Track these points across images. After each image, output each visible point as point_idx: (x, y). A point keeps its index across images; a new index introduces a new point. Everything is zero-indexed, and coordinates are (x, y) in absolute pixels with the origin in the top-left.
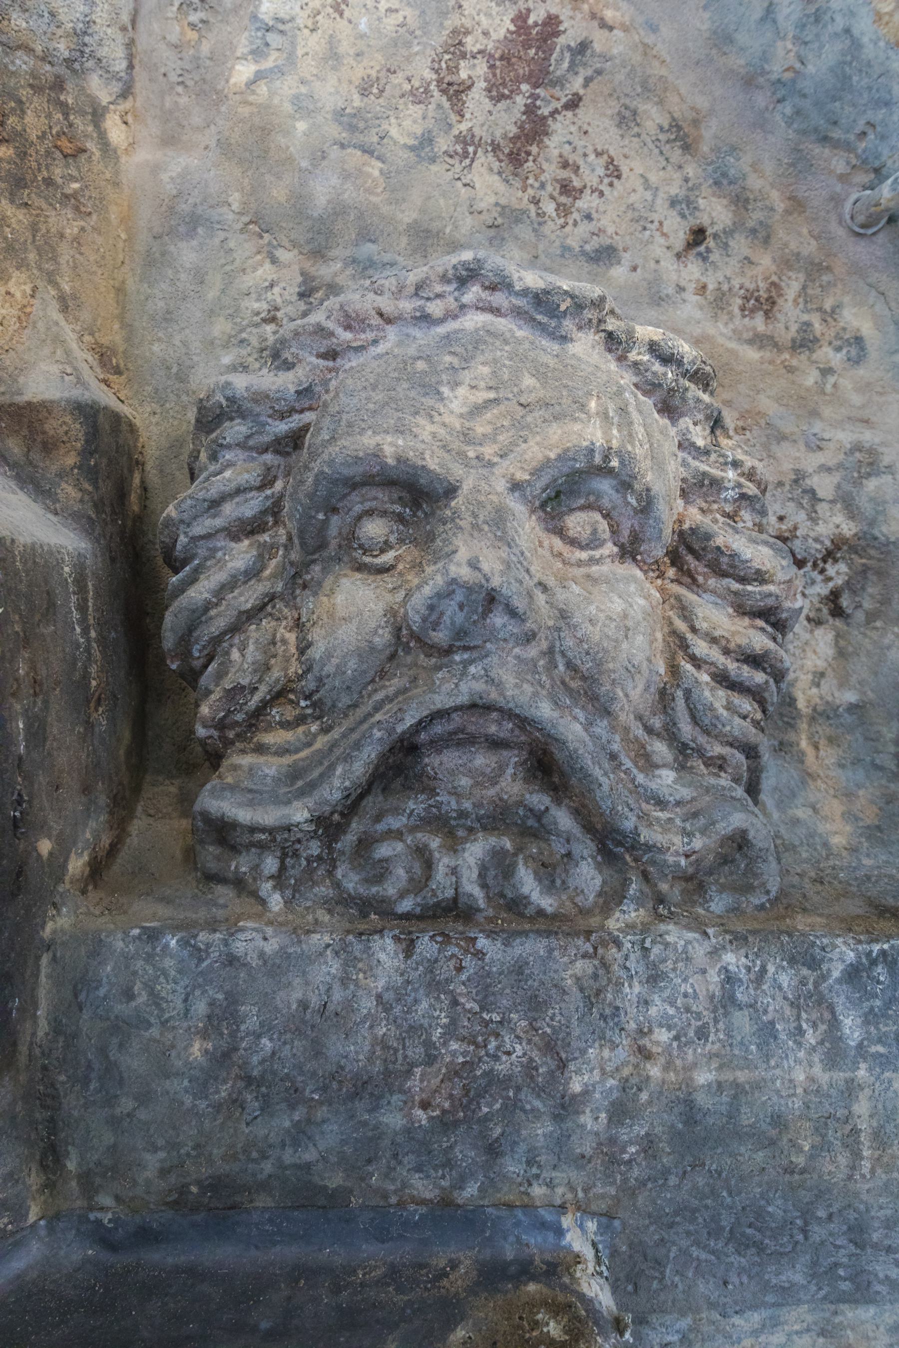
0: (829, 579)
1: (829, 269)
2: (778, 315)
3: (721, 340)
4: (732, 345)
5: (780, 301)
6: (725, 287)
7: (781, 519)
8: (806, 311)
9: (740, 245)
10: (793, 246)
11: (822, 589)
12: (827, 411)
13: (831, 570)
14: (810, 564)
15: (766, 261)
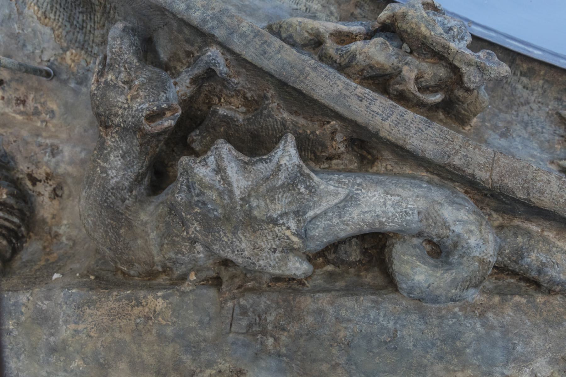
0: (51, 185)
1: (42, 90)
2: (28, 105)
3: (10, 114)
4: (13, 115)
5: (27, 101)
6: (10, 97)
7: (28, 168)
8: (36, 103)
9: (14, 84)
10: (30, 84)
11: (49, 189)
12: (44, 134)
13: (51, 183)
14: (43, 182)
15: (22, 89)
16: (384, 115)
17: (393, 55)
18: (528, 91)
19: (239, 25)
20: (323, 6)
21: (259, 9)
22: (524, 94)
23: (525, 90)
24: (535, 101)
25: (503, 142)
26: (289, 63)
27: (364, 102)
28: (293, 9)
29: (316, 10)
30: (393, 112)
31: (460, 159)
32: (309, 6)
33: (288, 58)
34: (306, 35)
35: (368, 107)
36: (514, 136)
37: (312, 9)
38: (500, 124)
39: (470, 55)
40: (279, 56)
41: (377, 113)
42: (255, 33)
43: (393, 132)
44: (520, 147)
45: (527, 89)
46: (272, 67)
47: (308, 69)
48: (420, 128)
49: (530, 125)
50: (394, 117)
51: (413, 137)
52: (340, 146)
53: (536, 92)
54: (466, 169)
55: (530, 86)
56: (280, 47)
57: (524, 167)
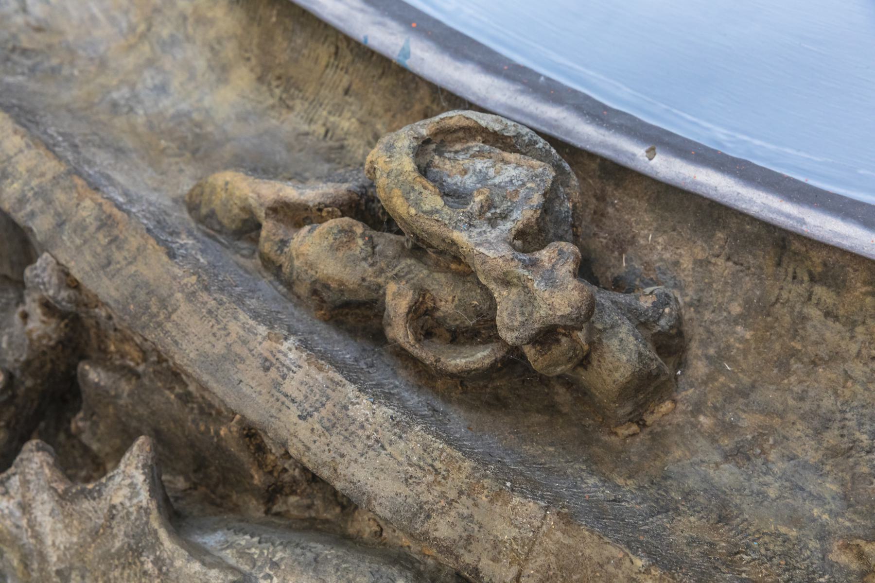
16: (306, 406)
17: (365, 259)
18: (838, 326)
19: (78, 205)
20: (362, 123)
21: (228, 140)
22: (828, 335)
23: (830, 322)
24: (859, 354)
25: (727, 475)
26: (147, 284)
27: (273, 373)
28: (299, 134)
29: (346, 134)
30: (328, 399)
31: (452, 525)
32: (333, 123)
33: (145, 272)
34: (236, 211)
35: (277, 385)
36: (772, 456)
37: (339, 133)
38: (749, 421)
39: (500, 261)
40: (132, 269)
41: (293, 401)
42: (101, 220)
43: (313, 447)
44: (772, 493)
45: (836, 318)
46: (113, 293)
47: (179, 295)
48: (377, 441)
49: (836, 425)
50: (324, 412)
51: (356, 461)
52: (286, 466)
53: (860, 329)
54: (462, 551)
55: (841, 312)
56: (138, 249)
57: (608, 559)
